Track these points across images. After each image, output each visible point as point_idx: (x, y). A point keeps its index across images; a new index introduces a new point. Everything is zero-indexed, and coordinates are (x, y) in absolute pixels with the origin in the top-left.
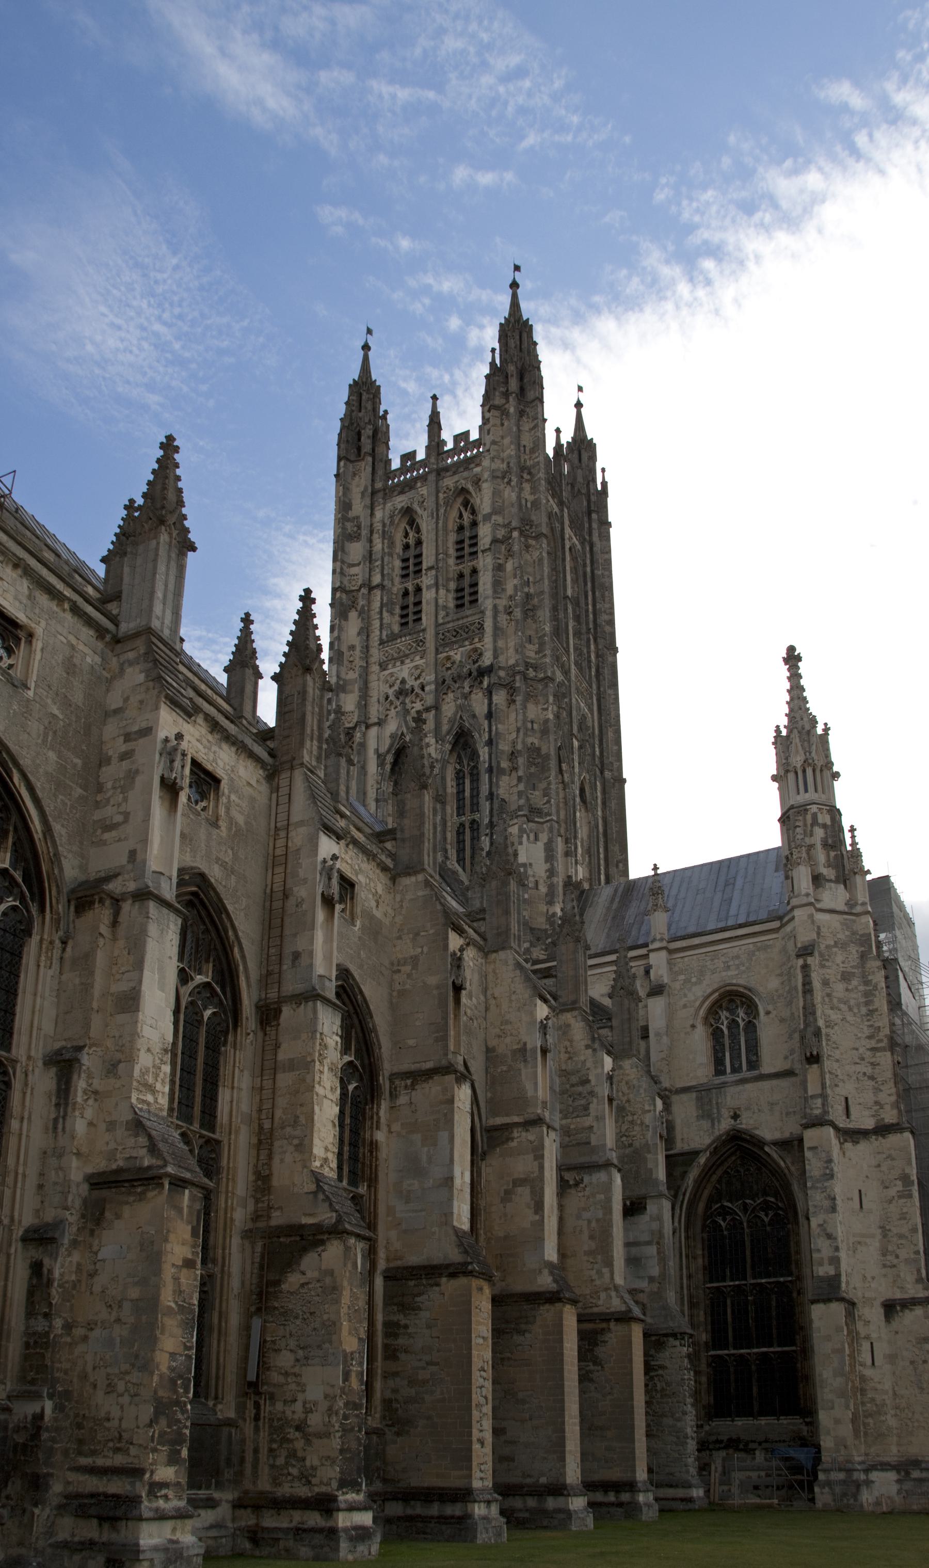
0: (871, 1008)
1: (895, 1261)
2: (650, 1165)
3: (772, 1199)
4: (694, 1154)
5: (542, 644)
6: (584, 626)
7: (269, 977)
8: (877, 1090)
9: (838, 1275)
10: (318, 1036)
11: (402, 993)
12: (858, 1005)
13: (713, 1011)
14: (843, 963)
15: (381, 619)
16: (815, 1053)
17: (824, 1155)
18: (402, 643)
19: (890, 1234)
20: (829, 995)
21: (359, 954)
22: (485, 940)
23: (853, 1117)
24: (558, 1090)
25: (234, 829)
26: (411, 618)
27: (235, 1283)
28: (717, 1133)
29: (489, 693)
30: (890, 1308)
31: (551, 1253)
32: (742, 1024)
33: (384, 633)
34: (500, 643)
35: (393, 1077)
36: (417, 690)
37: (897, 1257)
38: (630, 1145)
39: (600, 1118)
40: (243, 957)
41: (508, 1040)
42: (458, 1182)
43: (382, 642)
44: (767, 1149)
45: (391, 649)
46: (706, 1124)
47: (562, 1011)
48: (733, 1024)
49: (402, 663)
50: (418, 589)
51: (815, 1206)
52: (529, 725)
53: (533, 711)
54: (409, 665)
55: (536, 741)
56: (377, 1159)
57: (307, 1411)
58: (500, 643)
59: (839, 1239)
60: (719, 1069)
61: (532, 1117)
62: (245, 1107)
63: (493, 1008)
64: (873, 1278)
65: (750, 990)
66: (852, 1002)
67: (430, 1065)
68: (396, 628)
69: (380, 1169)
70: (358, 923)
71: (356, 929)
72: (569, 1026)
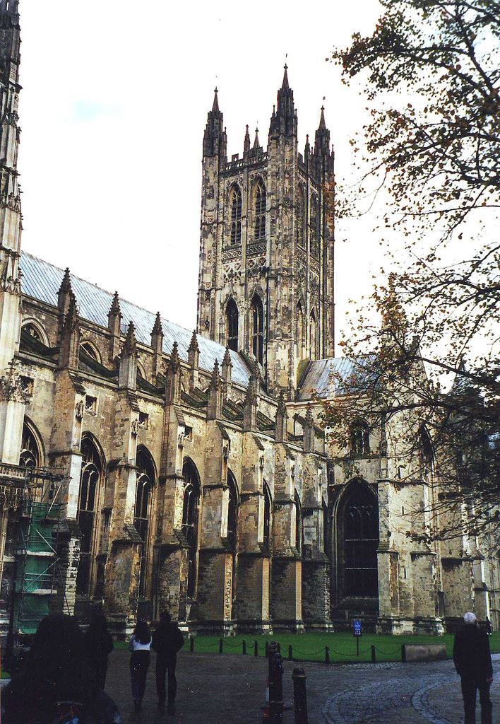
7: (163, 469)
11: (208, 459)
15: (223, 239)
18: (232, 252)
26: (236, 238)
27: (151, 562)
30: (414, 556)
31: (261, 538)
35: (204, 487)
42: (223, 522)
43: (223, 250)
50: (239, 224)
53: (285, 291)
57: (170, 598)
62: (155, 509)
68: (229, 243)
70: (193, 440)
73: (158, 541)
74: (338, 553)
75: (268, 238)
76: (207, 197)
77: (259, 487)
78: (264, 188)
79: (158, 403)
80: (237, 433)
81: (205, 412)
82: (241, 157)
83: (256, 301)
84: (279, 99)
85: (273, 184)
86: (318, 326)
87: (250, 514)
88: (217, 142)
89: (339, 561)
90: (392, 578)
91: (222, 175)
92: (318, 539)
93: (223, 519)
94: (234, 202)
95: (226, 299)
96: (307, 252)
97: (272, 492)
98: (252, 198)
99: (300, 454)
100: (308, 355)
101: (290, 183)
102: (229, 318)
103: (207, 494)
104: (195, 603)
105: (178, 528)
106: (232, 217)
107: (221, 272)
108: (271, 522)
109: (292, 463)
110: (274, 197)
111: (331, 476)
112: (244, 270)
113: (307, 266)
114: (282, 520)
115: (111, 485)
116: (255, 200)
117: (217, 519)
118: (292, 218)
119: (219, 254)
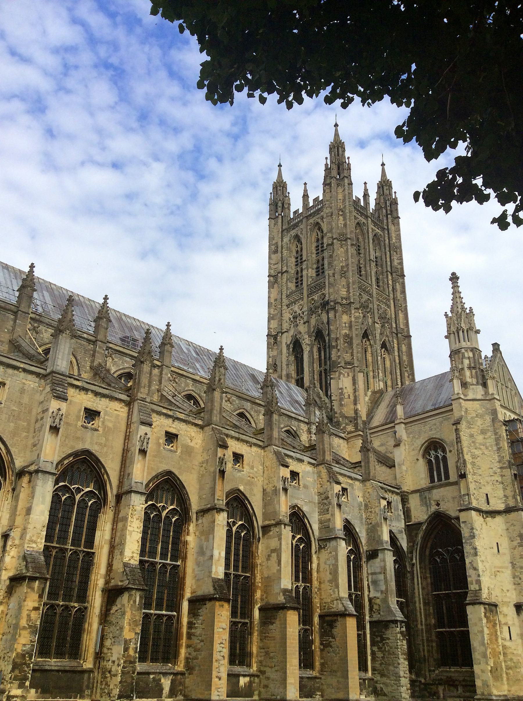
0: (499, 447)
1: (520, 582)
2: (379, 533)
3: (459, 547)
4: (420, 524)
5: (348, 288)
6: (385, 269)
7: (121, 483)
8: (505, 489)
9: (480, 589)
10: (131, 507)
12: (491, 446)
13: (426, 452)
14: (481, 425)
16: (463, 473)
17: (469, 525)
19: (516, 566)
20: (473, 442)
21: (179, 463)
22: (263, 442)
23: (490, 504)
24: (317, 502)
25: (106, 429)
26: (300, 283)
28: (430, 513)
29: (328, 313)
32: (440, 457)
33: (288, 292)
37: (520, 579)
38: (371, 523)
39: (333, 515)
40: (108, 477)
41: (270, 485)
44: (453, 521)
46: (424, 509)
47: (318, 465)
48: (437, 458)
49: (295, 304)
51: (467, 553)
52: (344, 325)
55: (347, 332)
56: (186, 548)
58: (331, 290)
59: (480, 571)
60: (432, 480)
61: (278, 520)
63: (265, 471)
64: (508, 591)
65: (441, 440)
66: (488, 444)
67: (209, 506)
68: (294, 288)
69: (188, 553)
70: (179, 451)
71: (177, 453)
72: (320, 472)
73: (107, 582)
74: (425, 610)
75: (326, 273)
78: (322, 232)
79: (117, 399)
80: (254, 449)
84: (330, 152)
85: (329, 223)
87: (273, 551)
89: (426, 620)
90: (490, 639)
92: (387, 589)
93: (216, 553)
94: (297, 252)
95: (292, 340)
96: (371, 285)
97: (316, 527)
99: (357, 483)
101: (345, 219)
102: (296, 357)
103: (200, 521)
104: (182, 674)
105: (132, 562)
108: (315, 566)
109: (337, 488)
111: (407, 514)
112: (305, 309)
113: (372, 297)
114: (328, 562)
115: (16, 498)
116: (315, 245)
117: (208, 554)
118: (347, 249)
119: (284, 300)
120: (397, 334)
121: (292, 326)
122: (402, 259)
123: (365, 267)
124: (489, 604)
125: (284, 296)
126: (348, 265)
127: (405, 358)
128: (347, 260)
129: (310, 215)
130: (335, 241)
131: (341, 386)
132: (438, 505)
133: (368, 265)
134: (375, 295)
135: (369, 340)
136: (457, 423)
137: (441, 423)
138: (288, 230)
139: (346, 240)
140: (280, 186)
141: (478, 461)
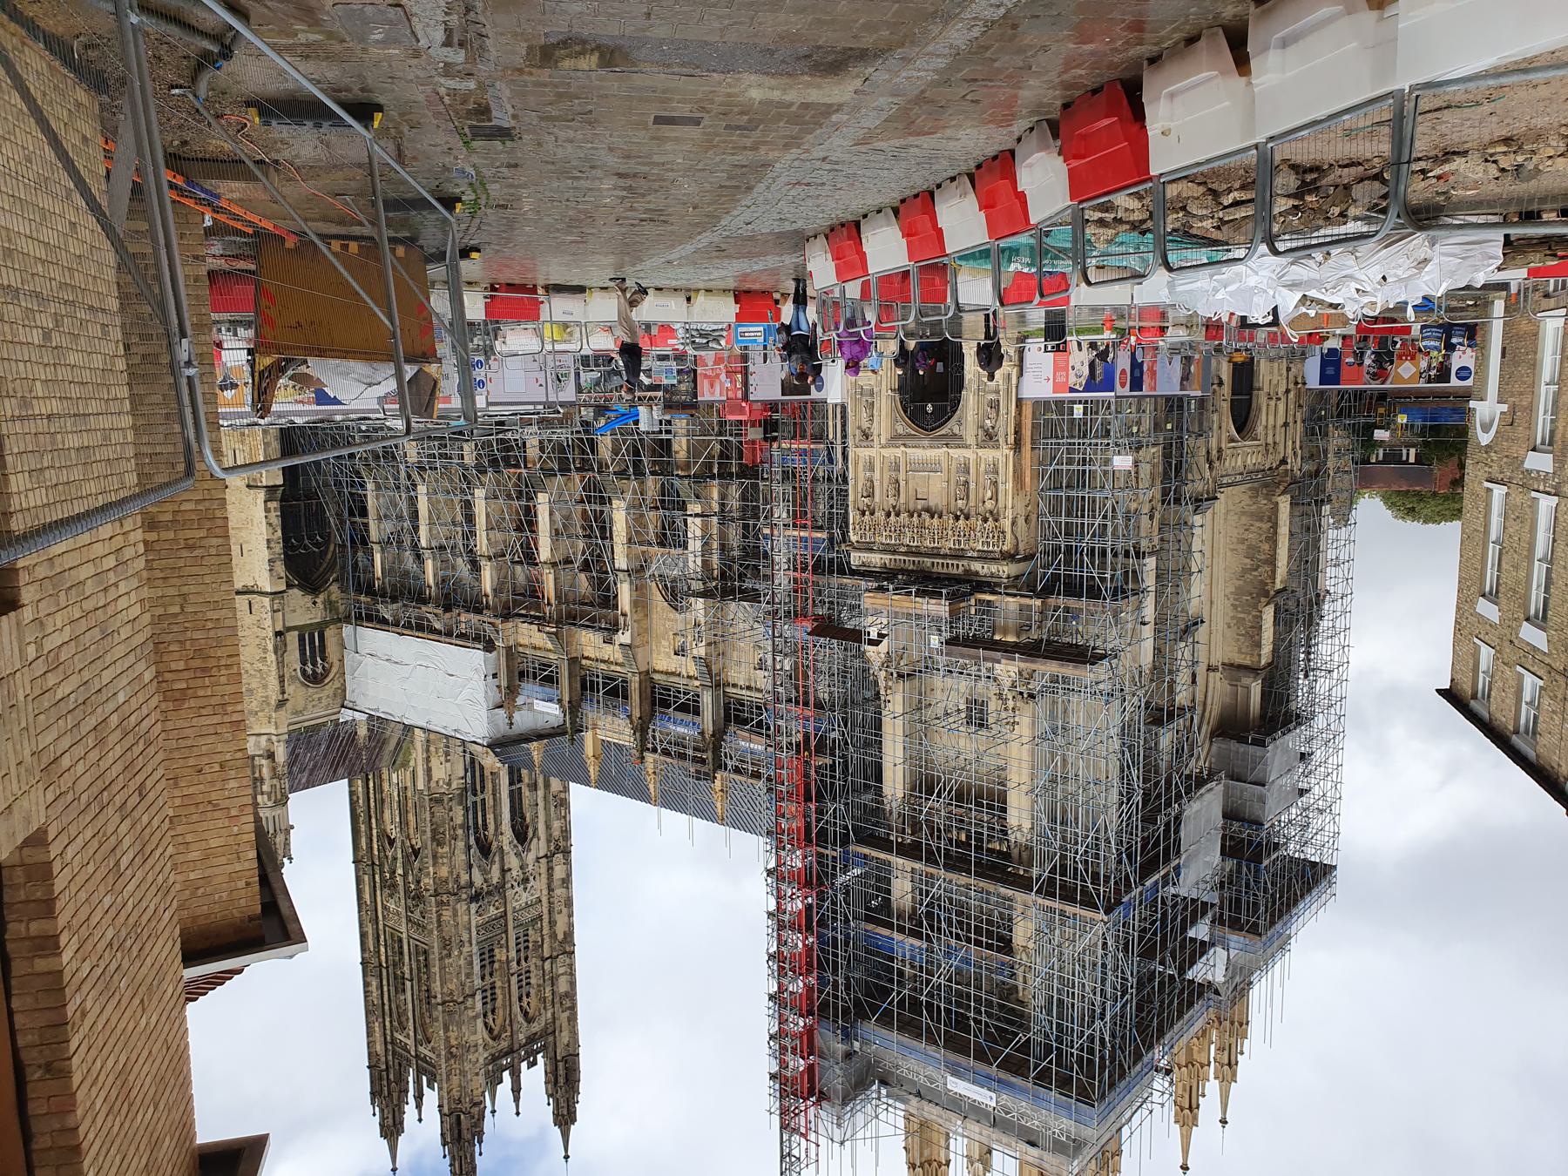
5: (439, 921)
9: (265, 502)
13: (326, 672)
15: (542, 936)
18: (527, 916)
26: (521, 940)
34: (466, 918)
36: (515, 884)
43: (541, 917)
45: (533, 913)
48: (314, 664)
50: (518, 963)
54: (522, 902)
58: (466, 918)
68: (531, 932)
75: (475, 949)
76: (571, 995)
77: (488, 568)
78: (486, 1024)
81: (582, 668)
82: (524, 1065)
83: (485, 849)
86: (380, 821)
88: (561, 1080)
91: (550, 1031)
94: (528, 995)
96: (409, 937)
98: (504, 1006)
100: (394, 776)
101: (447, 1039)
102: (523, 818)
106: (529, 972)
107: (539, 886)
110: (471, 1013)
112: (510, 893)
116: (499, 1002)
118: (442, 985)
119: (545, 911)
120: (373, 863)
121: (530, 867)
122: (365, 992)
123: (419, 970)
124: (257, 487)
125: (546, 917)
126: (441, 959)
127: (363, 827)
128: (442, 968)
129: (506, 1055)
130: (461, 999)
131: (448, 764)
132: (315, 603)
133: (415, 971)
134: (404, 920)
135: (412, 846)
136: (281, 704)
137: (305, 708)
138: (544, 1033)
139: (443, 1003)
140: (563, 1116)
141: (259, 653)
